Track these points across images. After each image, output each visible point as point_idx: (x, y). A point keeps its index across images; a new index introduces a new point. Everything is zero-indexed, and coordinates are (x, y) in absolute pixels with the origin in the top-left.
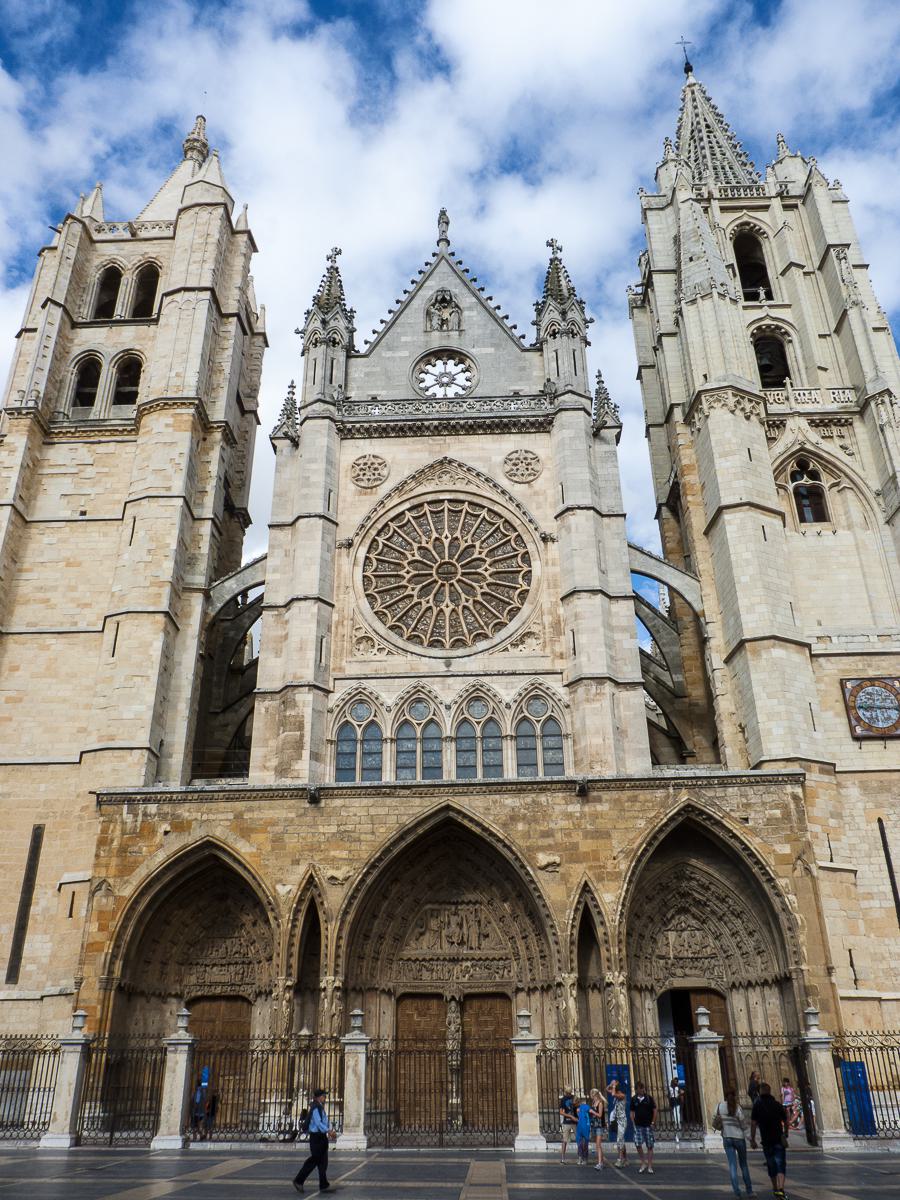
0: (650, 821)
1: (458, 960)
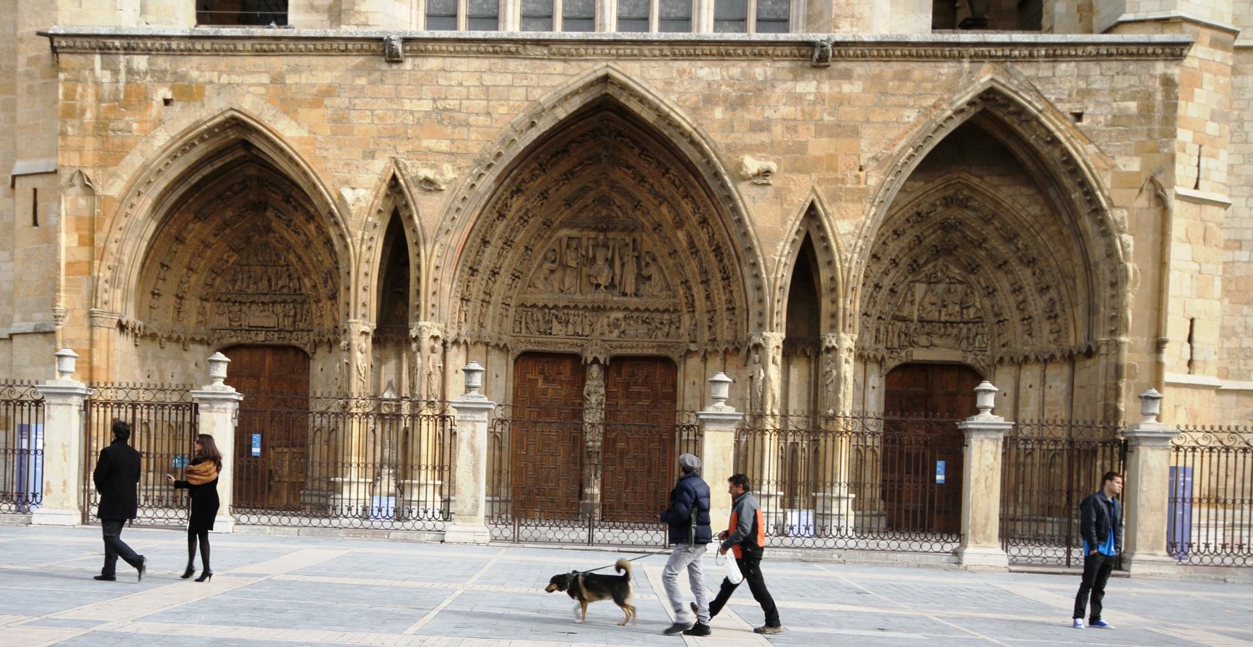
0: (925, 112)
1: (605, 309)
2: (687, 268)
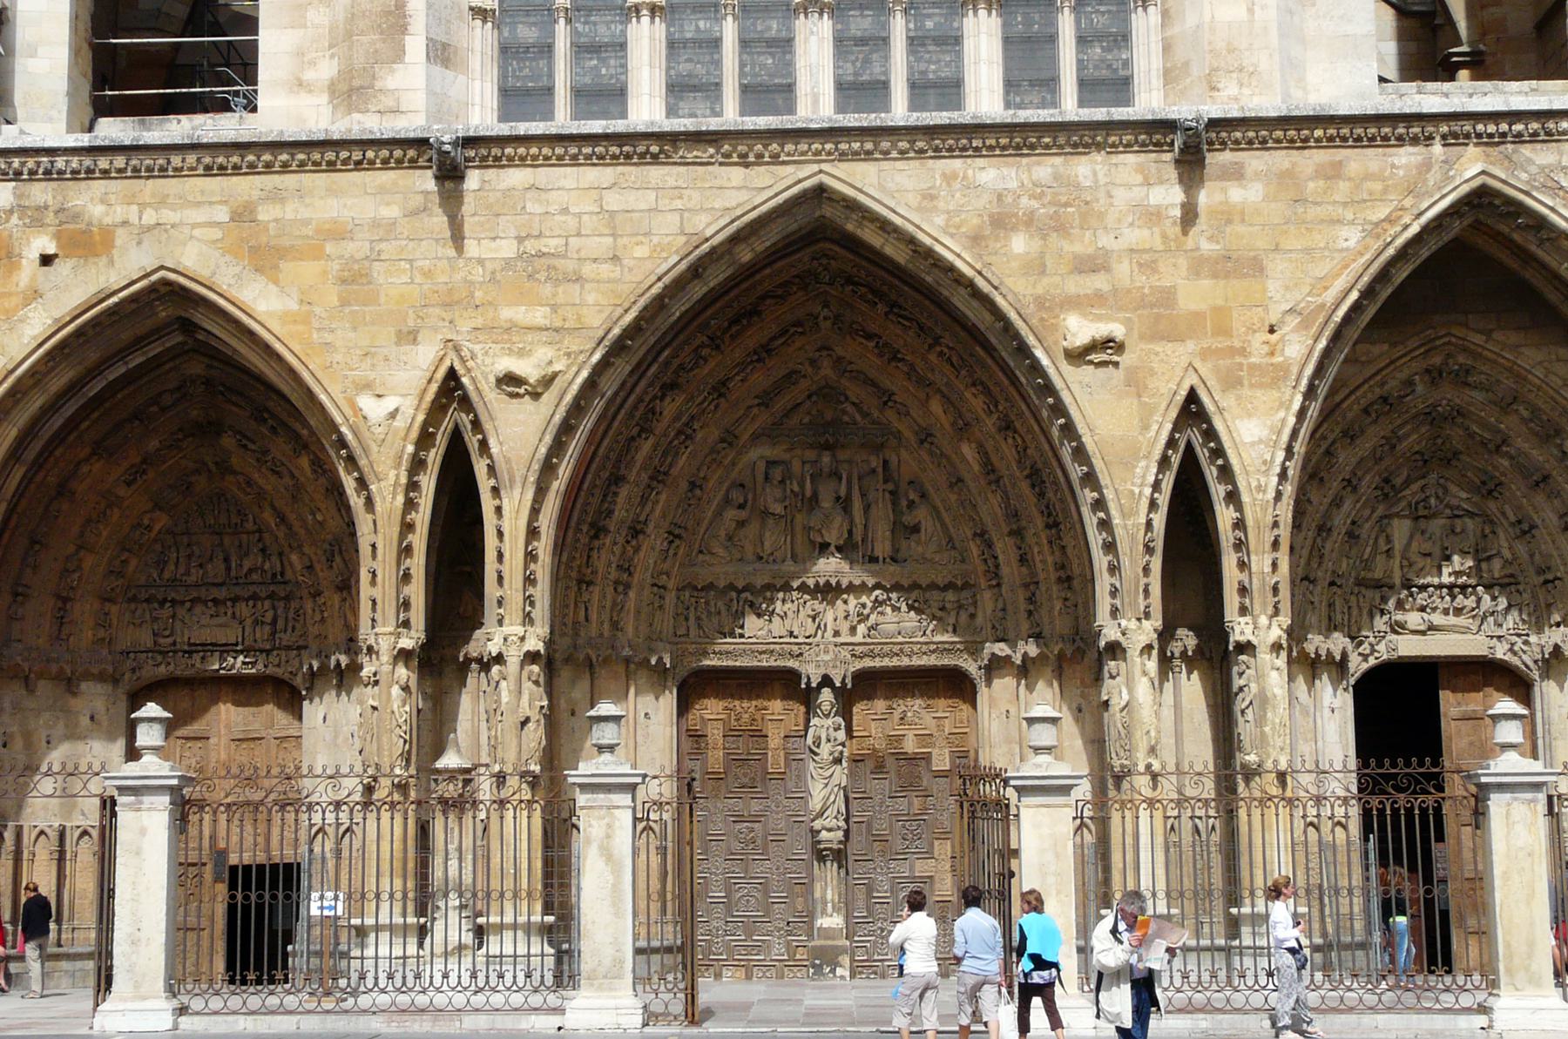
2: (984, 510)
